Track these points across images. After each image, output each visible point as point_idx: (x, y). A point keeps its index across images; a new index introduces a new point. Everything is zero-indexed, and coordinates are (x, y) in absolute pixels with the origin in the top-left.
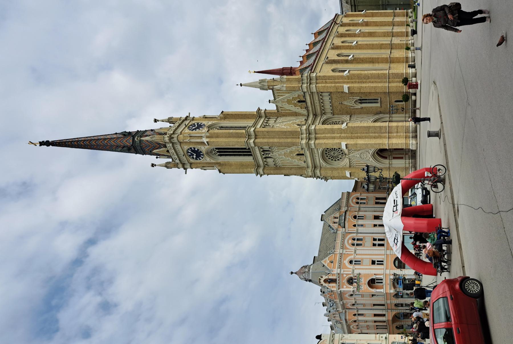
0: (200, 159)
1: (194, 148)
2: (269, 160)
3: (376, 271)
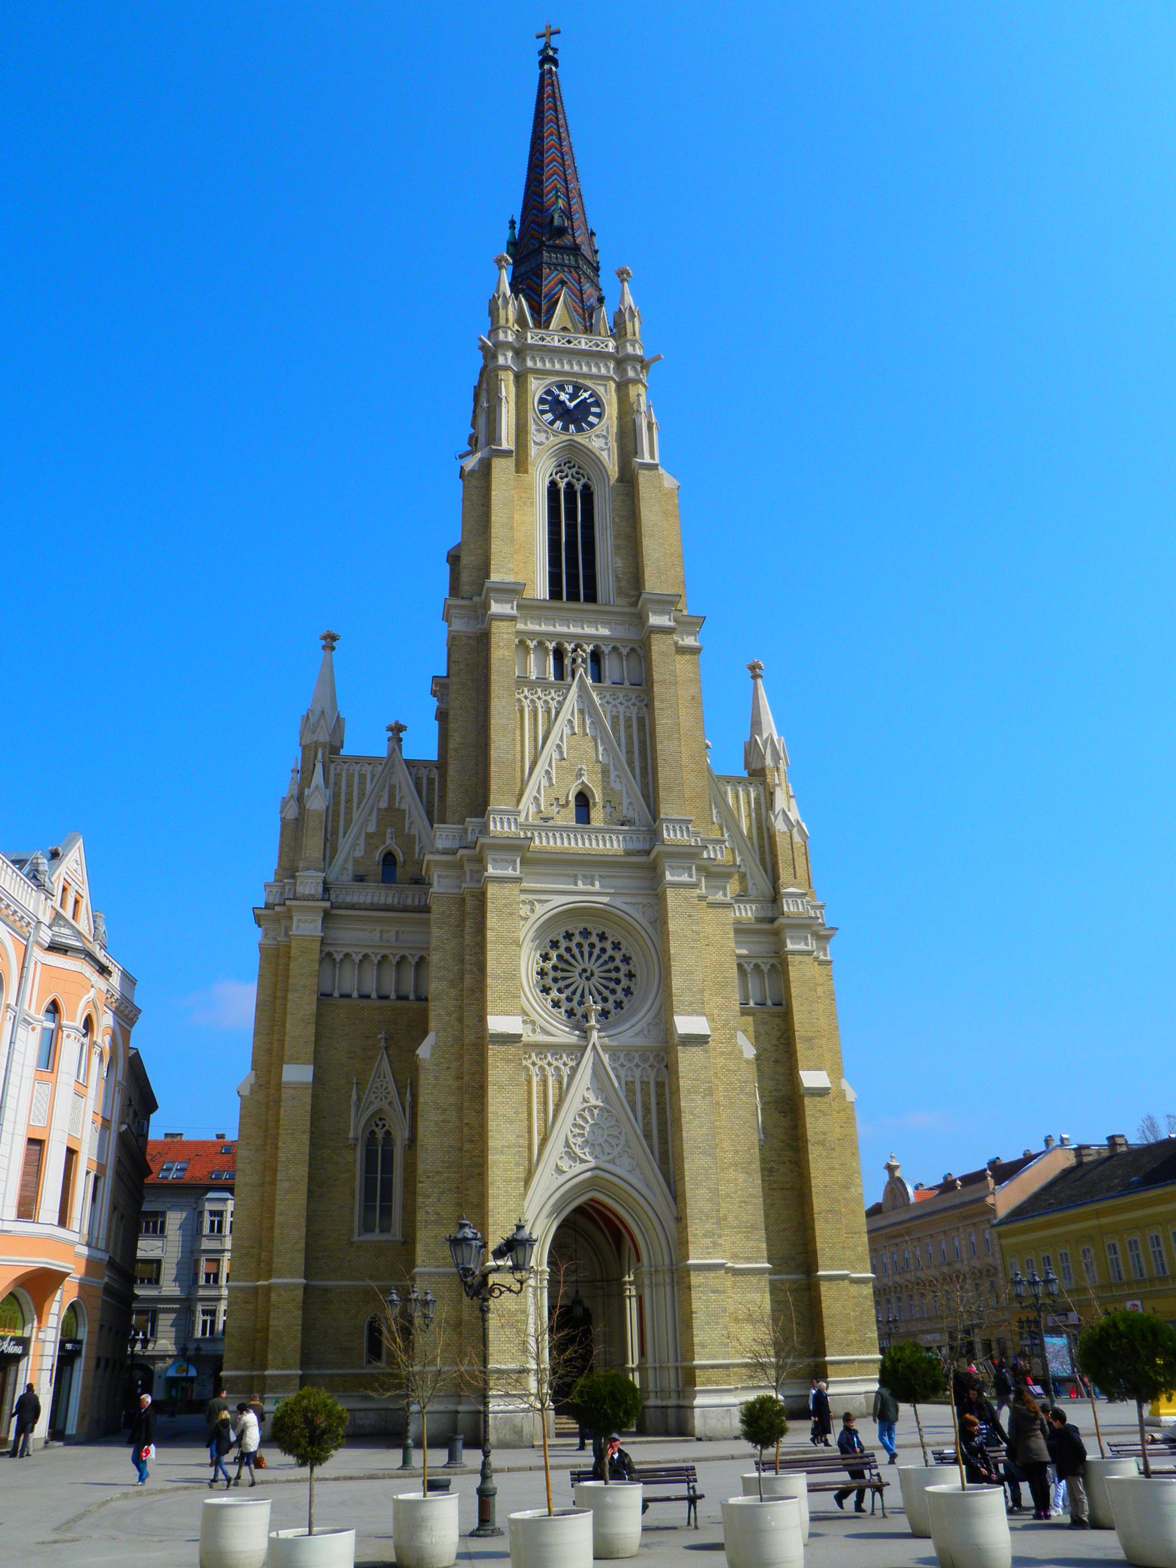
0: (543, 412)
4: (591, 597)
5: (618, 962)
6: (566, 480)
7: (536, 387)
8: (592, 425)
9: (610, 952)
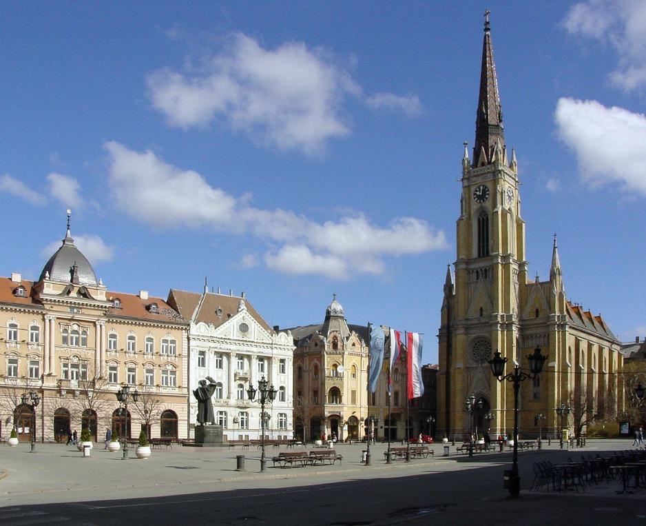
1: (488, 190)
3: (346, 396)
8: (487, 198)
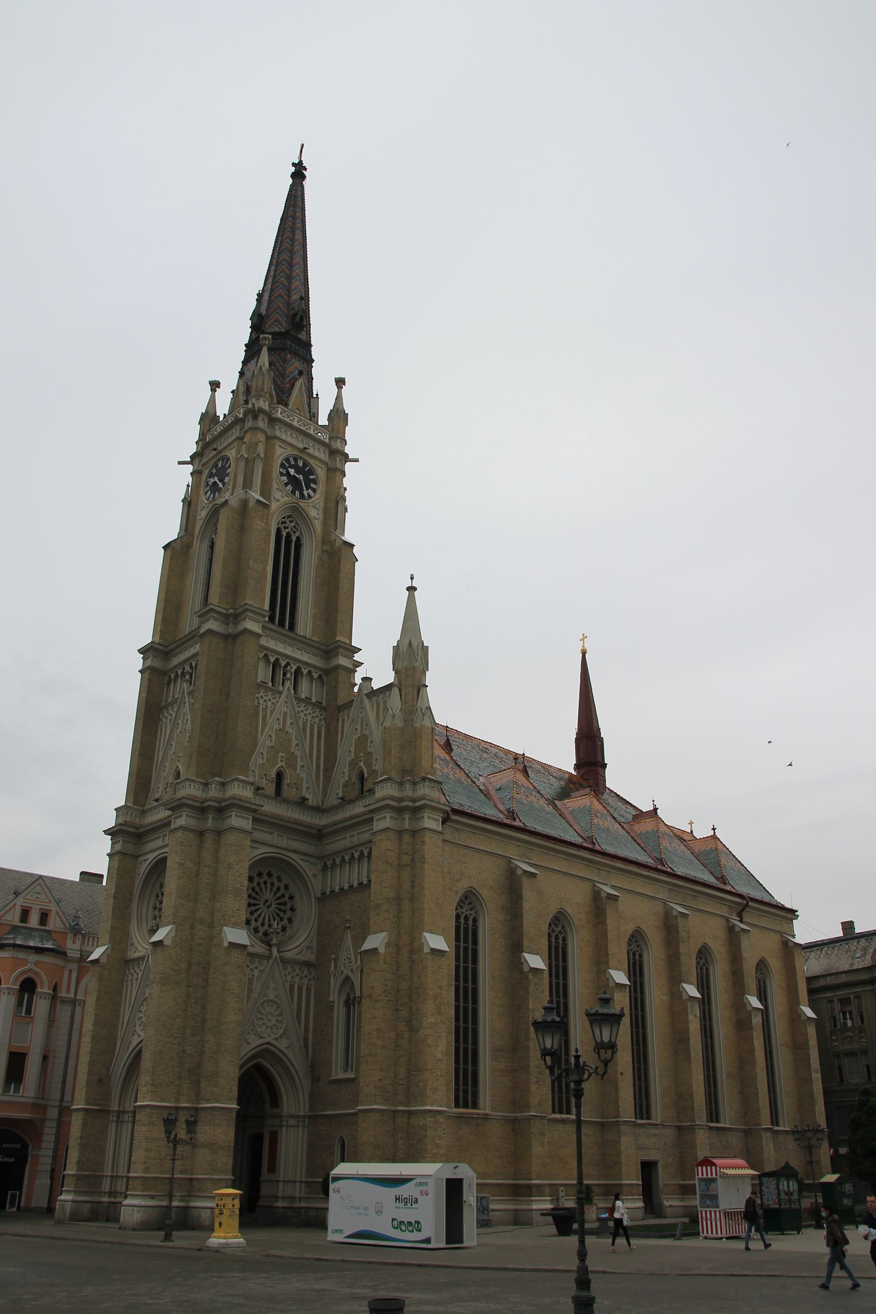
0: (282, 474)
1: (314, 481)
2: (263, 673)
4: (292, 627)
5: (286, 898)
6: (287, 530)
7: (280, 453)
9: (283, 890)
